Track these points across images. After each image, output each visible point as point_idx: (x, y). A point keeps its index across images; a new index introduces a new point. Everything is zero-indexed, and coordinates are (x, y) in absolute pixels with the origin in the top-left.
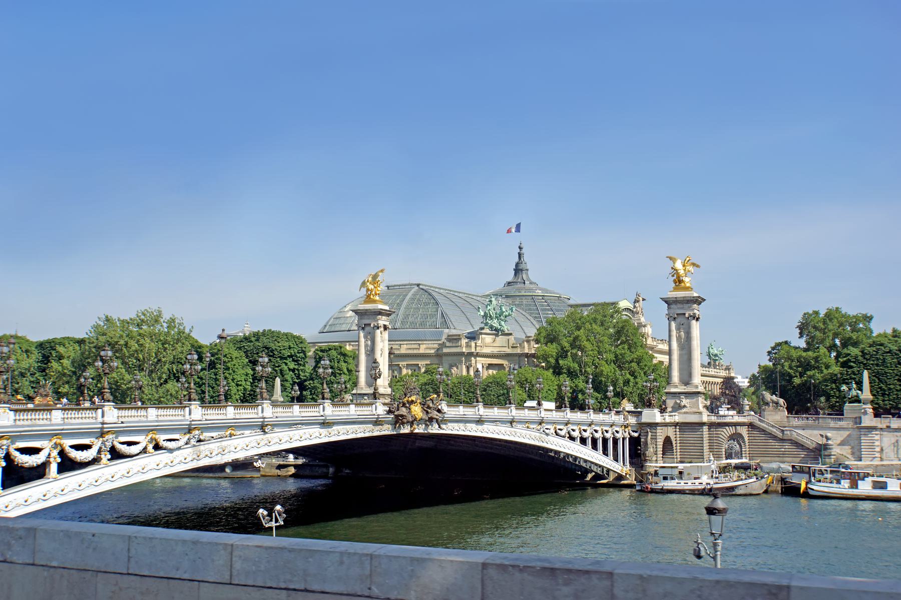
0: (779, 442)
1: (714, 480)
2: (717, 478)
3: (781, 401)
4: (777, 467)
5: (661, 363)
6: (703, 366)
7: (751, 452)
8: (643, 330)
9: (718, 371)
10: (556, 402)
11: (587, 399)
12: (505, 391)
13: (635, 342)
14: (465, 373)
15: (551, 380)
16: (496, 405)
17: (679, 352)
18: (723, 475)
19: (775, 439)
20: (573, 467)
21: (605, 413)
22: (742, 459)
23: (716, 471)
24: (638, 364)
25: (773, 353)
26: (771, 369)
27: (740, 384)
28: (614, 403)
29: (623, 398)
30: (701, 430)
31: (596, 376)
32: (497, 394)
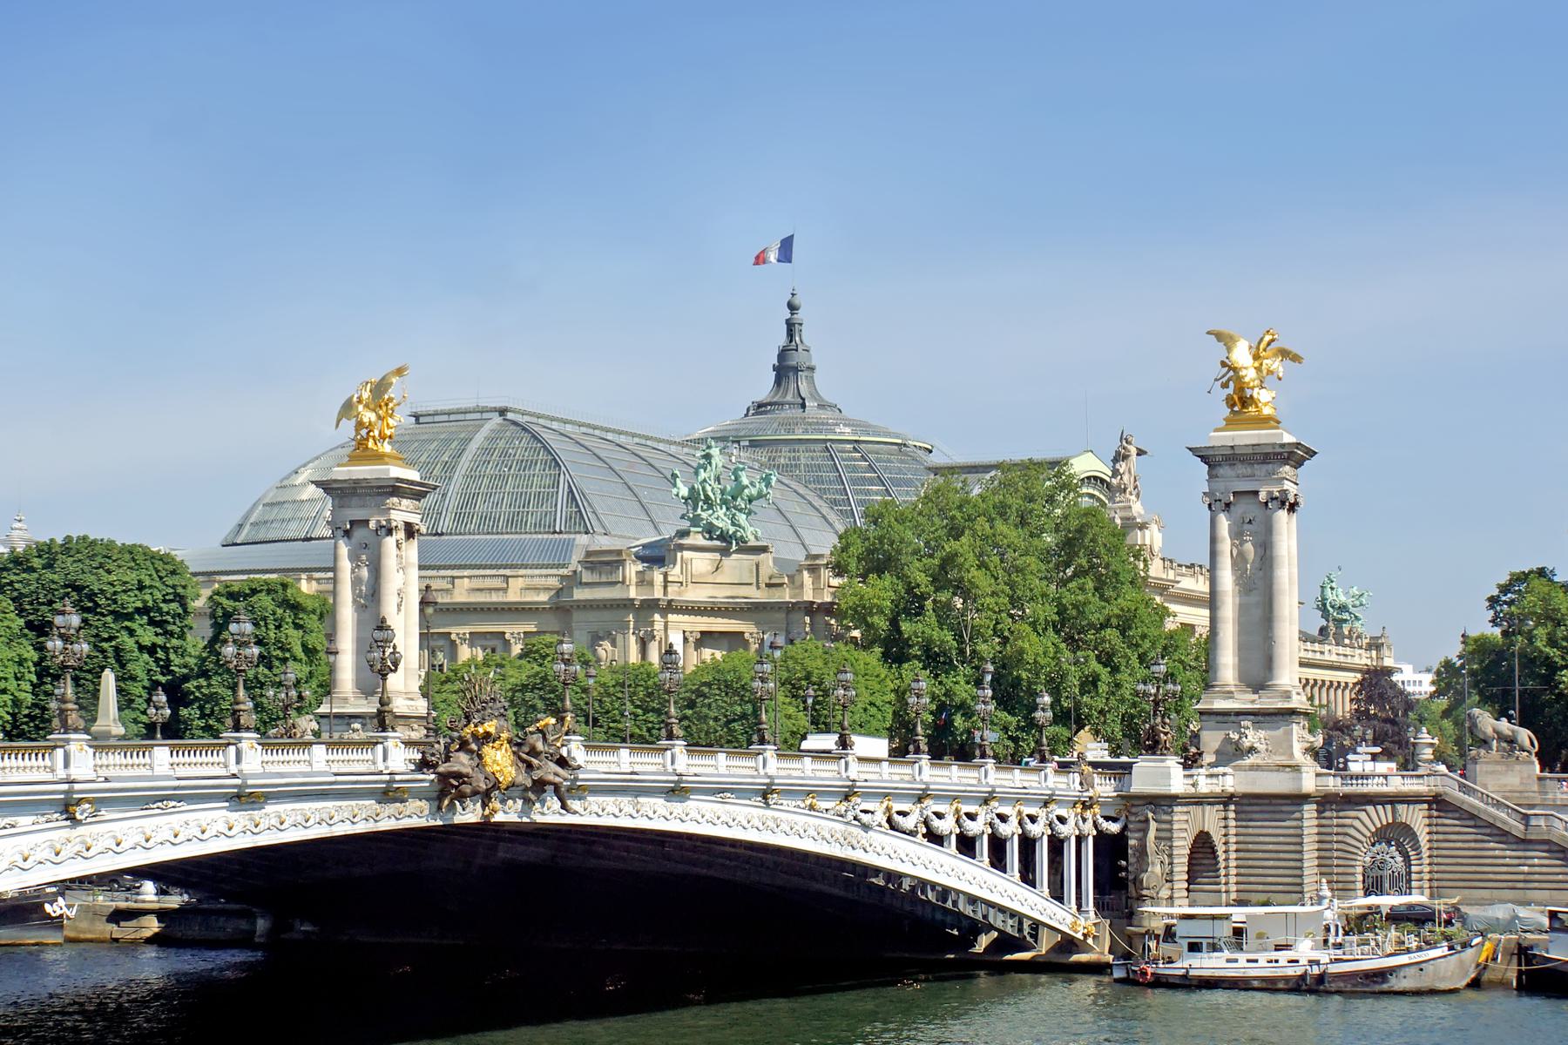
0: (1514, 847)
1: (1332, 951)
2: (1339, 946)
3: (1524, 735)
4: (1507, 916)
5: (1189, 628)
6: (1305, 637)
7: (1436, 876)
8: (1139, 537)
9: (1348, 651)
10: (891, 739)
11: (978, 729)
12: (749, 708)
13: (1114, 572)
14: (634, 657)
15: (878, 676)
16: (722, 747)
17: (1237, 599)
18: (1355, 938)
19: (1504, 839)
20: (939, 916)
21: (1027, 769)
22: (1410, 894)
23: (1337, 926)
24: (1123, 633)
25: (1505, 603)
26: (1496, 645)
27: (1410, 689)
28: (1054, 740)
29: (1081, 727)
30: (1297, 815)
31: (1004, 665)
32: (726, 716)
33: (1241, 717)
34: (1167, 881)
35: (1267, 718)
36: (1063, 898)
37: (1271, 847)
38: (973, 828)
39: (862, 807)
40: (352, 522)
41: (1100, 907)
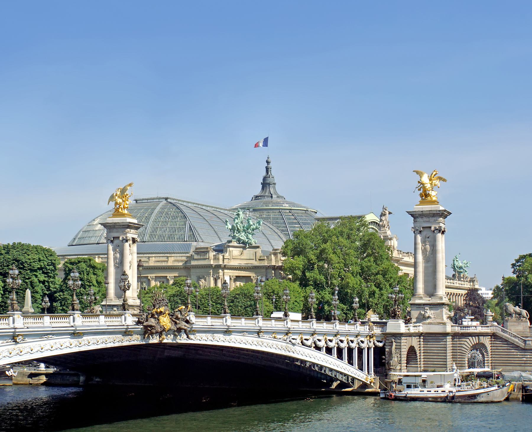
0: (521, 351)
1: (457, 388)
2: (459, 386)
3: (524, 312)
4: (519, 376)
5: (407, 275)
6: (447, 278)
7: (493, 361)
8: (389, 243)
9: (463, 283)
10: (302, 314)
11: (333, 310)
12: (253, 303)
13: (380, 255)
14: (212, 285)
15: (298, 292)
16: (243, 316)
17: (424, 265)
18: (465, 383)
19: (517, 348)
20: (319, 376)
21: (350, 324)
22: (484, 368)
23: (459, 379)
24: (384, 276)
25: (518, 266)
26: (514, 281)
27: (484, 296)
28: (359, 314)
29: (369, 309)
30: (445, 340)
31: (342, 288)
32: (245, 306)
33: (425, 306)
34: (399, 363)
35: (434, 306)
36: (363, 369)
37: (435, 351)
38: (331, 345)
39: (292, 338)
40: (114, 238)
41: (375, 372)
